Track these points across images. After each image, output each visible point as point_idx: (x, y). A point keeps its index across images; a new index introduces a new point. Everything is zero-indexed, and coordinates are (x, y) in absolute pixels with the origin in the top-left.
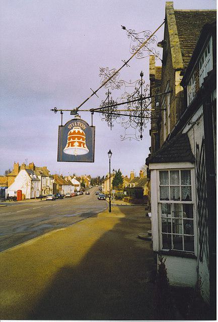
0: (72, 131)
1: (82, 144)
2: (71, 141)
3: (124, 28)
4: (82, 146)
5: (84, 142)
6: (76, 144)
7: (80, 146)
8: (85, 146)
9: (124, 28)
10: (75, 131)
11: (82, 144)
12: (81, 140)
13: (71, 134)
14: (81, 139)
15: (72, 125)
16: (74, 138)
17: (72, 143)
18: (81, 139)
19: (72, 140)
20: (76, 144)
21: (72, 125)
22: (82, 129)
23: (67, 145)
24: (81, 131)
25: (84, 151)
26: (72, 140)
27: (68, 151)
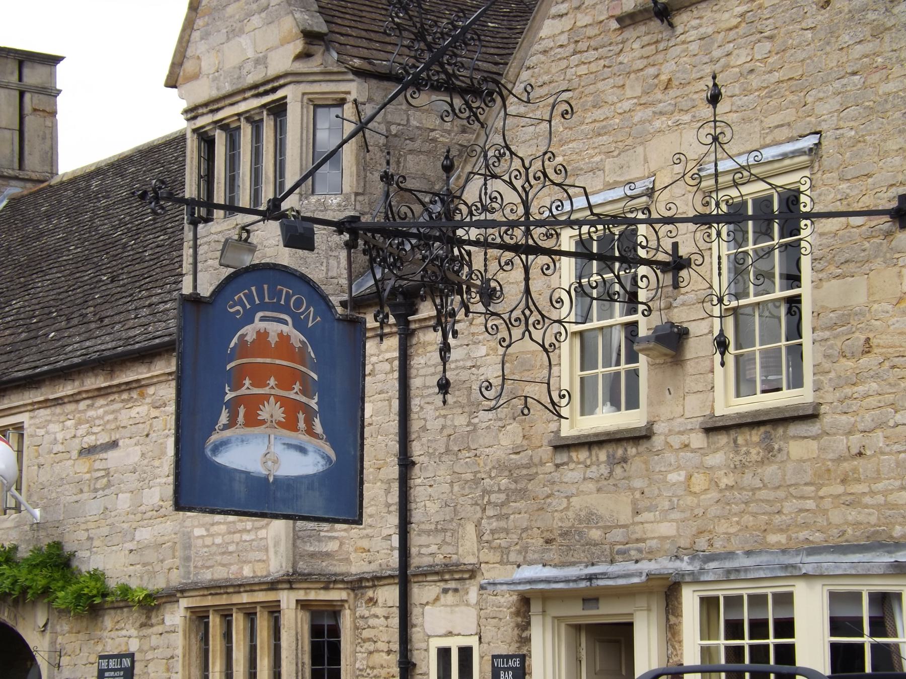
0: (249, 332)
1: (301, 416)
2: (243, 391)
4: (302, 425)
5: (313, 403)
6: (271, 411)
7: (290, 424)
8: (318, 428)
10: (262, 336)
11: (301, 416)
13: (244, 349)
14: (297, 387)
16: (259, 376)
17: (253, 403)
18: (297, 387)
19: (247, 388)
20: (271, 411)
22: (299, 325)
23: (224, 418)
24: (297, 337)
25: (298, 460)
26: (247, 388)
27: (245, 453)
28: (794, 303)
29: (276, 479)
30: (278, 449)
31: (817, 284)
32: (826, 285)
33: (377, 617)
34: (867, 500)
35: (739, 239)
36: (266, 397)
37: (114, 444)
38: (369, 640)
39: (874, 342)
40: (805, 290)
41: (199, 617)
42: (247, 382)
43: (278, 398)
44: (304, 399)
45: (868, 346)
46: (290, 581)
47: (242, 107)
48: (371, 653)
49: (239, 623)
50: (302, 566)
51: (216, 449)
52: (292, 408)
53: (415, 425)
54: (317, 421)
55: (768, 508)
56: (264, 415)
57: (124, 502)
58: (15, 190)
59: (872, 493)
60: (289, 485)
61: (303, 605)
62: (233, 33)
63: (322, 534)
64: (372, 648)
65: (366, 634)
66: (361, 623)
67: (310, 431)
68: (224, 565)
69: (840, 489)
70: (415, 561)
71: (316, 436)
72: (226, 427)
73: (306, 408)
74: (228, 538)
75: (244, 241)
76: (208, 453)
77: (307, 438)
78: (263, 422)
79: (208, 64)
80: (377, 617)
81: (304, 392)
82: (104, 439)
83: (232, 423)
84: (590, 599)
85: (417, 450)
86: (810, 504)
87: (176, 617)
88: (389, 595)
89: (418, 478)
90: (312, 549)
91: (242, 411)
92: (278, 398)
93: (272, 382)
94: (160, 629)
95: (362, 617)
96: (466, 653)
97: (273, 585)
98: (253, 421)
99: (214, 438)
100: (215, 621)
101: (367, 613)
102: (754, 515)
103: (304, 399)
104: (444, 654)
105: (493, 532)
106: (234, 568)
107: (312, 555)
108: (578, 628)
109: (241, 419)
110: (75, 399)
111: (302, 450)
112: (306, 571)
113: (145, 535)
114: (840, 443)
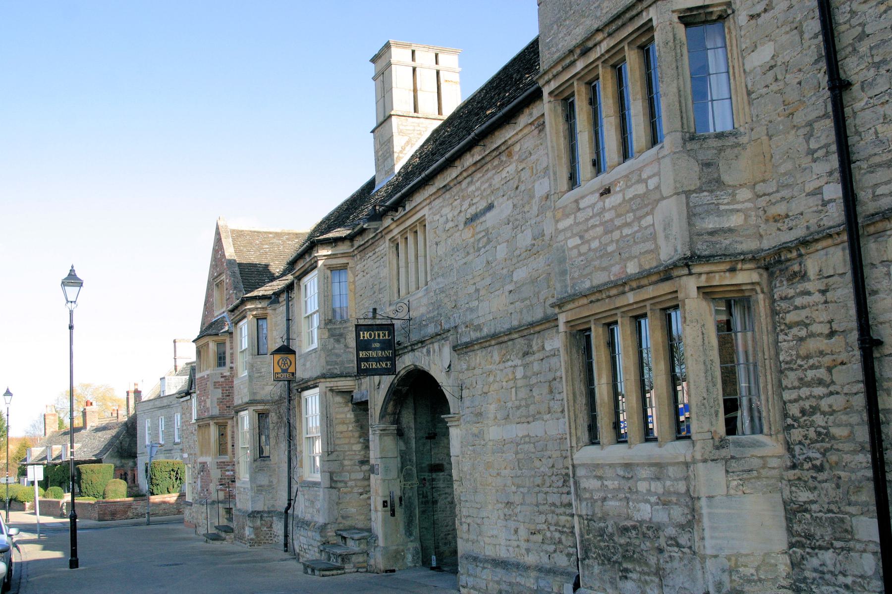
33: (809, 293)
37: (490, 207)
38: (797, 324)
41: (581, 338)
46: (689, 262)
48: (801, 339)
49: (623, 335)
50: (702, 248)
53: (846, 37)
57: (502, 251)
61: (706, 292)
63: (722, 207)
64: (803, 333)
65: (791, 317)
66: (784, 305)
68: (604, 269)
70: (867, 205)
74: (606, 239)
80: (809, 293)
82: (483, 205)
85: (853, 68)
87: (556, 342)
88: (836, 258)
89: (858, 103)
90: (711, 226)
95: (784, 299)
97: (666, 274)
100: (598, 336)
101: (791, 292)
106: (616, 269)
110: (457, 181)
112: (707, 253)
113: (520, 274)
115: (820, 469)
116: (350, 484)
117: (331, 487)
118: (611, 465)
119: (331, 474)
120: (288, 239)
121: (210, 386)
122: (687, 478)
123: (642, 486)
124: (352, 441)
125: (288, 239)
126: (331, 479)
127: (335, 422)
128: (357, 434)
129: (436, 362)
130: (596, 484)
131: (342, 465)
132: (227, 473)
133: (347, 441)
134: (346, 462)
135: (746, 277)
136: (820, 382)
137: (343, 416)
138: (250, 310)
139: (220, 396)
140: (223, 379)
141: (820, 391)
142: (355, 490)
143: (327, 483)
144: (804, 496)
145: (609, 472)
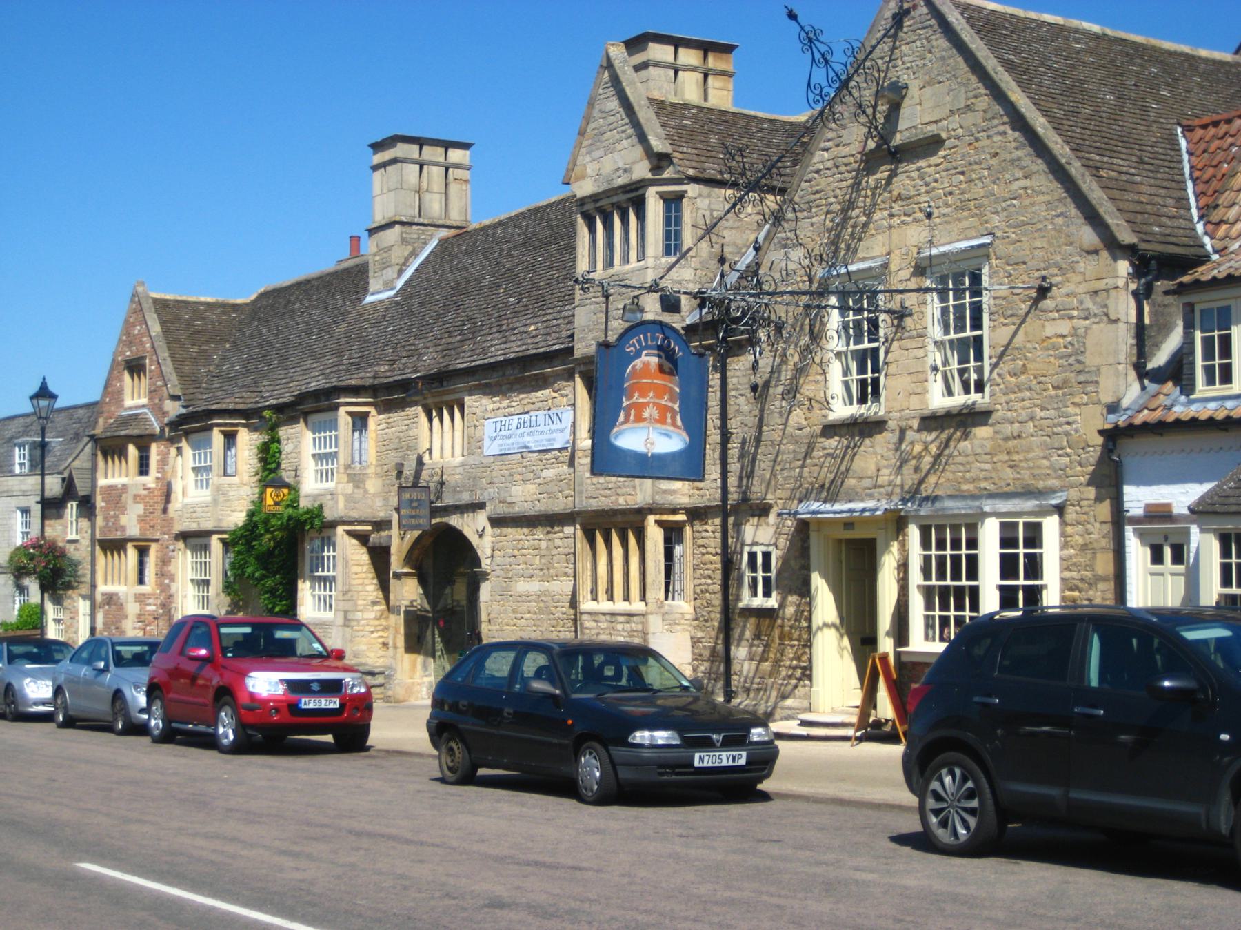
0: (638, 363)
3: (792, 16)
4: (669, 420)
5: (676, 407)
7: (662, 421)
8: (679, 422)
9: (792, 16)
11: (669, 415)
12: (665, 401)
15: (639, 342)
17: (639, 408)
19: (636, 398)
21: (639, 342)
23: (622, 418)
28: (978, 341)
29: (653, 455)
30: (654, 436)
31: (993, 329)
32: (998, 330)
33: (706, 531)
34: (1023, 464)
35: (944, 299)
36: (648, 404)
39: (1028, 366)
40: (985, 332)
42: (636, 395)
43: (655, 404)
44: (670, 404)
45: (1024, 370)
47: (615, 199)
50: (659, 499)
51: (616, 437)
52: (663, 410)
53: (731, 410)
54: (678, 418)
55: (961, 468)
56: (646, 414)
58: (444, 233)
59: (1026, 460)
60: (661, 459)
61: (659, 523)
62: (609, 150)
64: (704, 551)
65: (700, 542)
67: (674, 424)
69: (1006, 458)
71: (678, 427)
72: (623, 423)
73: (672, 410)
75: (636, 306)
76: (612, 439)
77: (671, 428)
78: (645, 420)
79: (591, 169)
81: (672, 400)
83: (627, 420)
84: (848, 524)
86: (988, 466)
91: (633, 412)
92: (655, 404)
93: (651, 394)
94: (561, 535)
96: (767, 556)
98: (639, 419)
99: (615, 430)
102: (953, 472)
103: (670, 404)
104: (753, 556)
105: (785, 479)
106: (613, 498)
107: (665, 492)
108: (840, 541)
109: (632, 417)
111: (668, 436)
114: (1008, 429)
115: (706, 621)
116: (363, 622)
117: (345, 625)
118: (604, 614)
119: (346, 612)
120: (224, 313)
121: (127, 498)
122: (642, 623)
123: (620, 627)
124: (367, 581)
125: (224, 313)
126: (345, 618)
127: (351, 563)
128: (371, 575)
129: (472, 526)
130: (593, 624)
131: (356, 605)
132: (149, 608)
133: (360, 581)
134: (360, 602)
135: (681, 517)
136: (710, 577)
137: (357, 557)
138: (218, 425)
139: (142, 512)
140: (146, 492)
141: (709, 581)
142: (368, 628)
143: (340, 621)
144: (700, 634)
145: (603, 618)
